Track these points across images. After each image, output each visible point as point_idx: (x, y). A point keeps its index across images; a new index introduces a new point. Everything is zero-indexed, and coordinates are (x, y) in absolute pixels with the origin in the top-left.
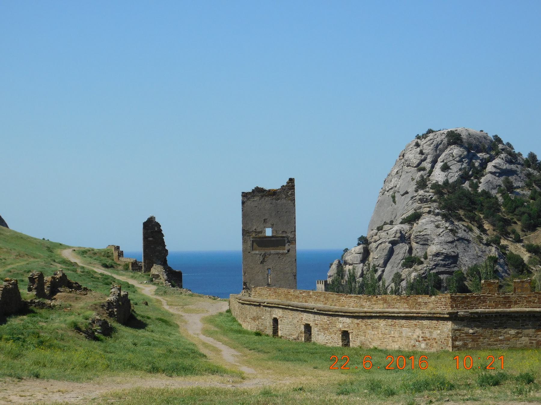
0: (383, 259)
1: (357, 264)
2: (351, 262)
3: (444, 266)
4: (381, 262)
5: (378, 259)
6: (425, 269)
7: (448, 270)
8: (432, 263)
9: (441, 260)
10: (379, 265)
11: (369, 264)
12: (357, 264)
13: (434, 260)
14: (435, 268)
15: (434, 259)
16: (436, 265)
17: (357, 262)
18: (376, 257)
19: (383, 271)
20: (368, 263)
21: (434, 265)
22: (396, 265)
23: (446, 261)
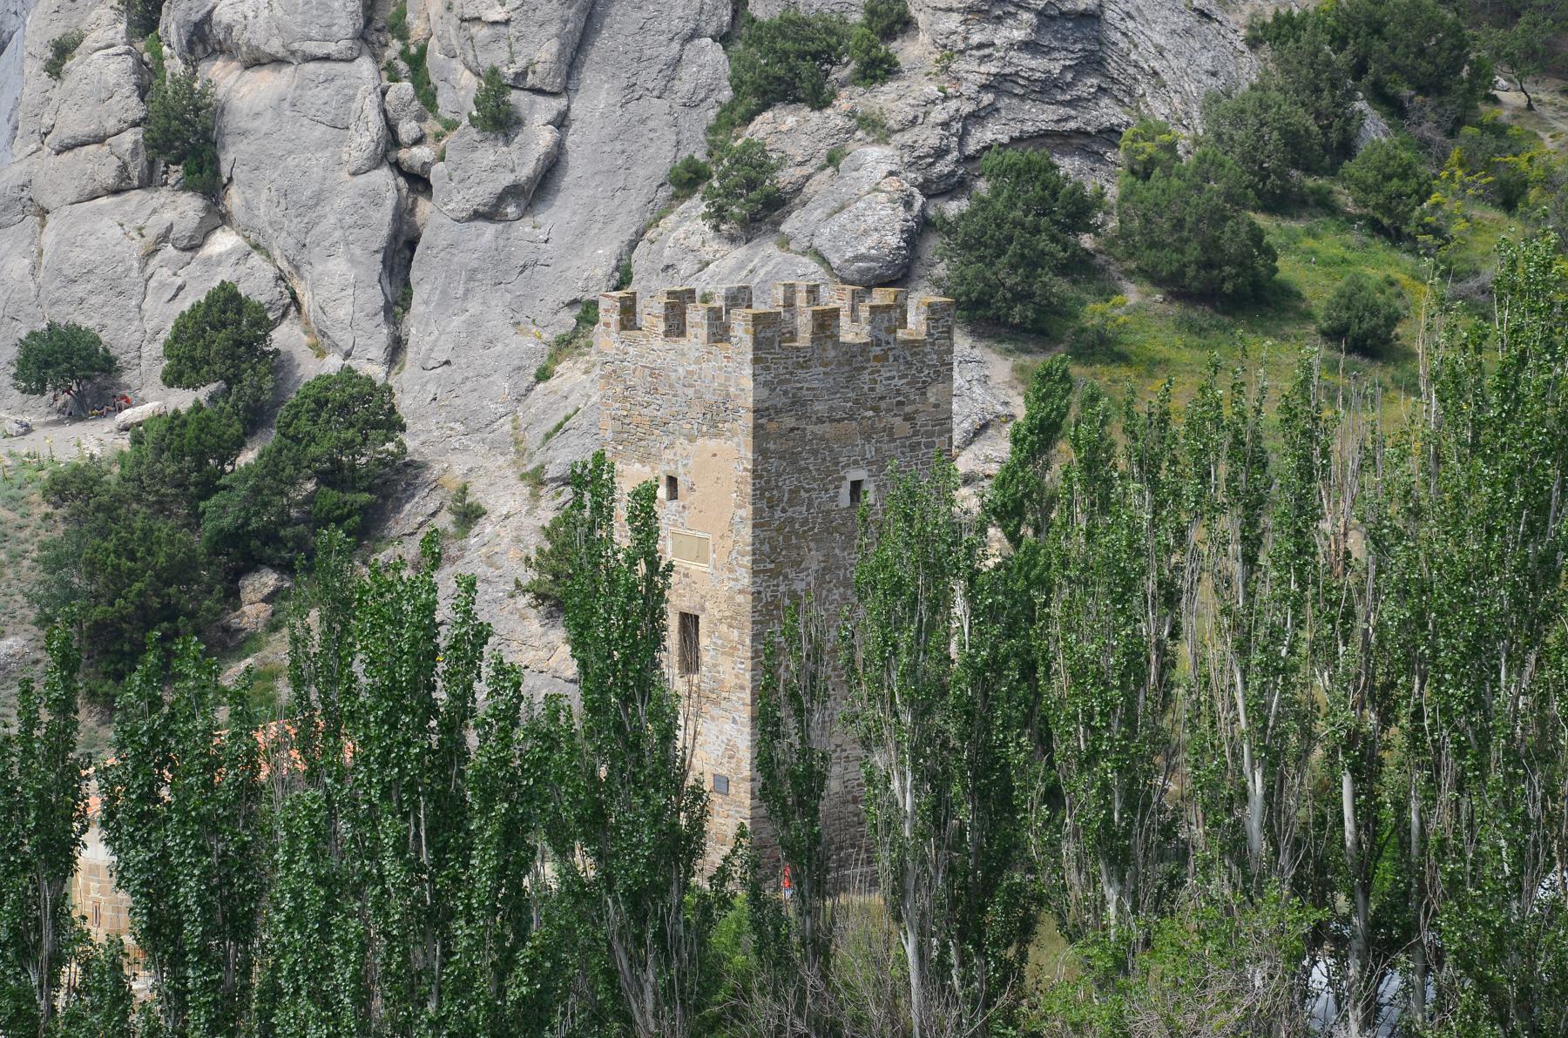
0: (553, 29)
1: (327, 58)
2: (275, 47)
3: (1045, 89)
4: (544, 51)
5: (512, 30)
6: (939, 114)
7: (1072, 125)
8: (974, 72)
9: (1028, 46)
10: (521, 75)
11: (417, 62)
12: (327, 58)
13: (980, 46)
14: (992, 110)
15: (976, 39)
16: (997, 85)
17: (331, 48)
18: (498, 14)
19: (561, 122)
20: (404, 54)
21: (984, 88)
22: (649, 78)
23: (1047, 51)
